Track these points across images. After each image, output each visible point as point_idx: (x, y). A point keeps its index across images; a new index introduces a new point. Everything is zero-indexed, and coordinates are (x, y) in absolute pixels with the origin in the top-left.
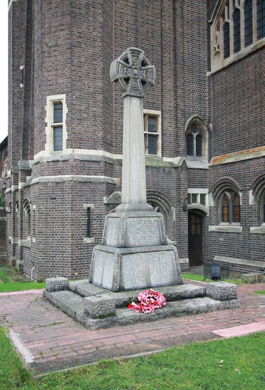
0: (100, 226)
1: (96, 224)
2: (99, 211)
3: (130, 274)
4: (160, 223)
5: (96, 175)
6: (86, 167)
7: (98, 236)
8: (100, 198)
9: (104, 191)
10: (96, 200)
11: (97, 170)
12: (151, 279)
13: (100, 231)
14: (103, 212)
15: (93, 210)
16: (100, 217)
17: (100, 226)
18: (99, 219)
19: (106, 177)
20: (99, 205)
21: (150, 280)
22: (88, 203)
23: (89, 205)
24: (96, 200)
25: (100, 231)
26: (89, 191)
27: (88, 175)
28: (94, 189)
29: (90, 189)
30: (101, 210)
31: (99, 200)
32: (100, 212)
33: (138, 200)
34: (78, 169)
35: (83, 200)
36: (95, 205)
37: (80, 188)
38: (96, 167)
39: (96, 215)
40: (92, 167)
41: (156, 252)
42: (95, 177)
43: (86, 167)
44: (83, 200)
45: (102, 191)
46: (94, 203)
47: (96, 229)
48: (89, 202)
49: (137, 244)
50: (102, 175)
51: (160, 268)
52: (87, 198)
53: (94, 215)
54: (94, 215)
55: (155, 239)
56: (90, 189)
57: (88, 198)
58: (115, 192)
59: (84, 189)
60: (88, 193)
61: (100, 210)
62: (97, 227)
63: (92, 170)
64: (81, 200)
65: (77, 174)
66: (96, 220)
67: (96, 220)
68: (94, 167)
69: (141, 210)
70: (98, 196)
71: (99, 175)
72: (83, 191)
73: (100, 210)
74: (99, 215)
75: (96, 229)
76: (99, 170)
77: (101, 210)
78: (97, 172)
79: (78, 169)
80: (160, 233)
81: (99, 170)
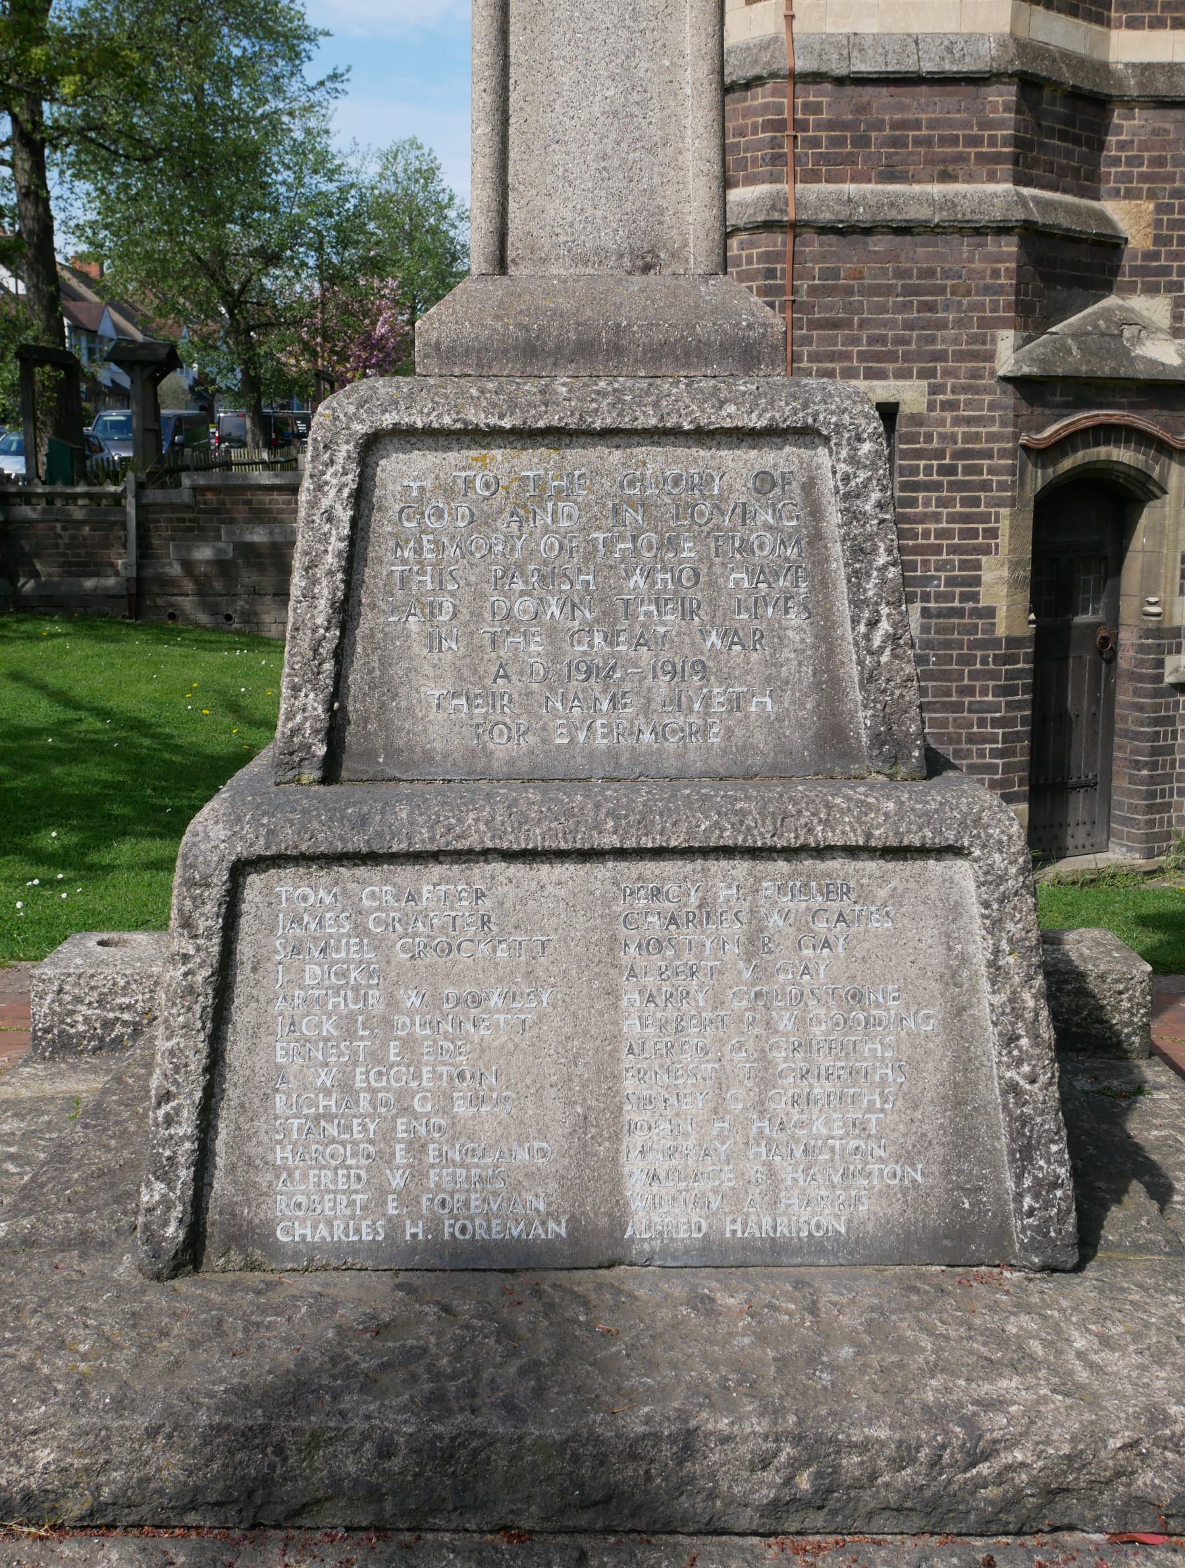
0: (965, 534)
1: (936, 517)
2: (960, 430)
3: (346, 1088)
4: (833, 517)
5: (946, 177)
6: (879, 125)
7: (949, 597)
8: (974, 340)
9: (1000, 290)
10: (940, 356)
11: (954, 141)
12: (634, 1169)
13: (964, 565)
14: (992, 437)
15: (916, 420)
16: (968, 470)
17: (965, 534)
18: (953, 486)
19: (1026, 191)
20: (965, 389)
21: (616, 1183)
22: (881, 375)
23: (884, 390)
24: (940, 356)
25: (964, 565)
26: (888, 290)
27: (890, 176)
28: (930, 273)
29: (901, 274)
30: (978, 421)
31: (960, 356)
32: (968, 438)
33: (611, 238)
34: (815, 142)
35: (846, 356)
36: (934, 390)
37: (825, 274)
38: (951, 124)
39: (939, 454)
40: (917, 125)
41: (717, 867)
42: (936, 189)
43: (879, 125)
44: (846, 356)
45: (987, 290)
46: (922, 375)
47: (937, 550)
48: (890, 366)
49: (501, 748)
50: (992, 178)
51: (764, 1062)
52: (872, 340)
53: (919, 454)
54: (919, 454)
55: (762, 704)
56: (901, 274)
57: (882, 340)
58: (1112, 301)
59: (860, 275)
60: (882, 309)
61: (969, 421)
62: (941, 534)
63: (918, 142)
64: (831, 357)
65: (812, 177)
66: (937, 486)
67: (937, 486)
68: (933, 124)
69: (616, 351)
70: (959, 323)
71: (971, 178)
72: (849, 291)
73: (969, 421)
74: (959, 455)
75: (937, 550)
76: (975, 141)
77: (978, 421)
78: (961, 158)
79: (815, 142)
80: (825, 635)
81: (975, 141)
